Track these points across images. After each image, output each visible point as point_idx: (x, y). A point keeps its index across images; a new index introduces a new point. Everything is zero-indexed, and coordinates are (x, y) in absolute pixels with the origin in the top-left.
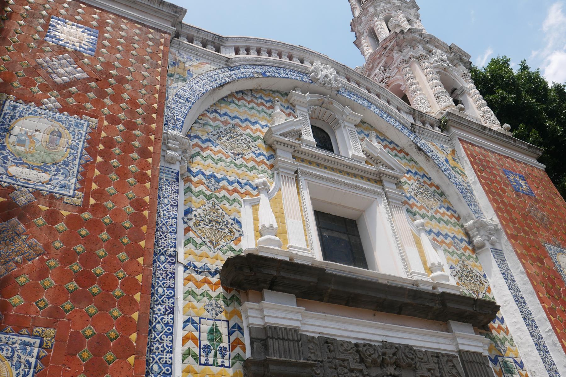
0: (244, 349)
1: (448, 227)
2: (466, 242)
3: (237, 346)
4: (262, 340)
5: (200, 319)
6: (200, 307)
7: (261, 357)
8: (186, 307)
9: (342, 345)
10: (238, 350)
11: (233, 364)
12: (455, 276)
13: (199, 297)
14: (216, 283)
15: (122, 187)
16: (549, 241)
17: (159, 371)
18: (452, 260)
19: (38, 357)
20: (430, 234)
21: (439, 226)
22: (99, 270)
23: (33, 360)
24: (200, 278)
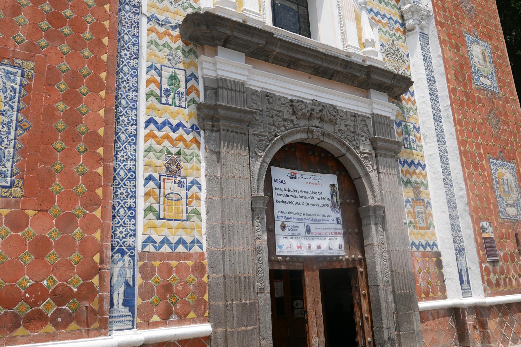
0: (198, 95)
1: (387, 8)
2: (400, 24)
3: (192, 92)
4: (213, 89)
5: (161, 66)
6: (162, 55)
7: (212, 102)
8: (149, 55)
9: (279, 99)
10: (193, 95)
11: (188, 106)
12: (383, 53)
13: (161, 47)
14: (176, 37)
16: (470, 32)
17: (127, 105)
18: (384, 39)
19: (21, 85)
20: (370, 13)
21: (379, 6)
23: (17, 87)
24: (162, 30)
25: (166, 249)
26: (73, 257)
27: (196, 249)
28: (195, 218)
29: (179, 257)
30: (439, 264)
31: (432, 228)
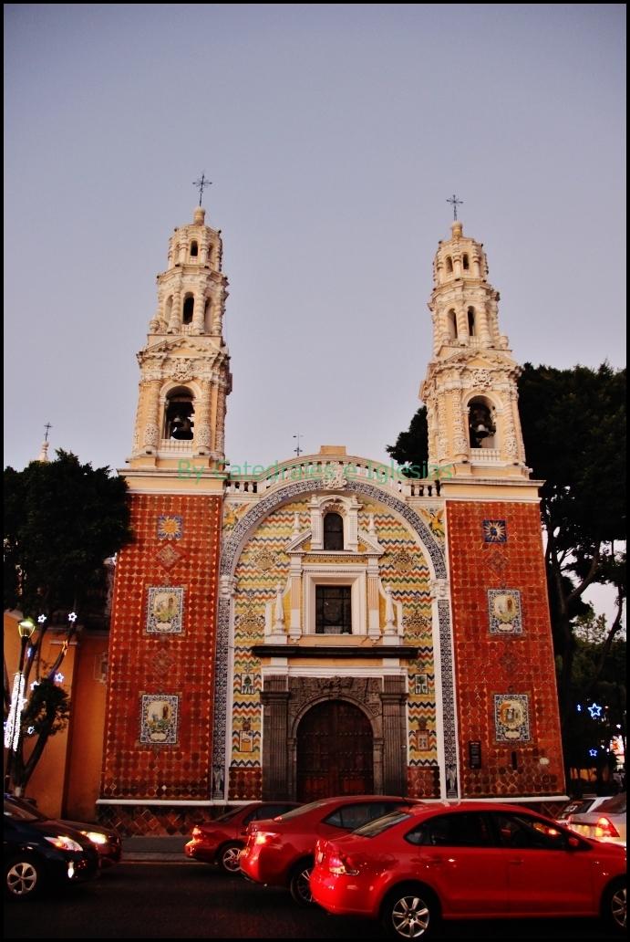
6: (241, 668)
10: (258, 686)
15: (201, 621)
22: (194, 666)
25: (242, 766)
26: (198, 770)
27: (257, 766)
28: (257, 751)
29: (248, 769)
30: (437, 775)
31: (433, 750)
